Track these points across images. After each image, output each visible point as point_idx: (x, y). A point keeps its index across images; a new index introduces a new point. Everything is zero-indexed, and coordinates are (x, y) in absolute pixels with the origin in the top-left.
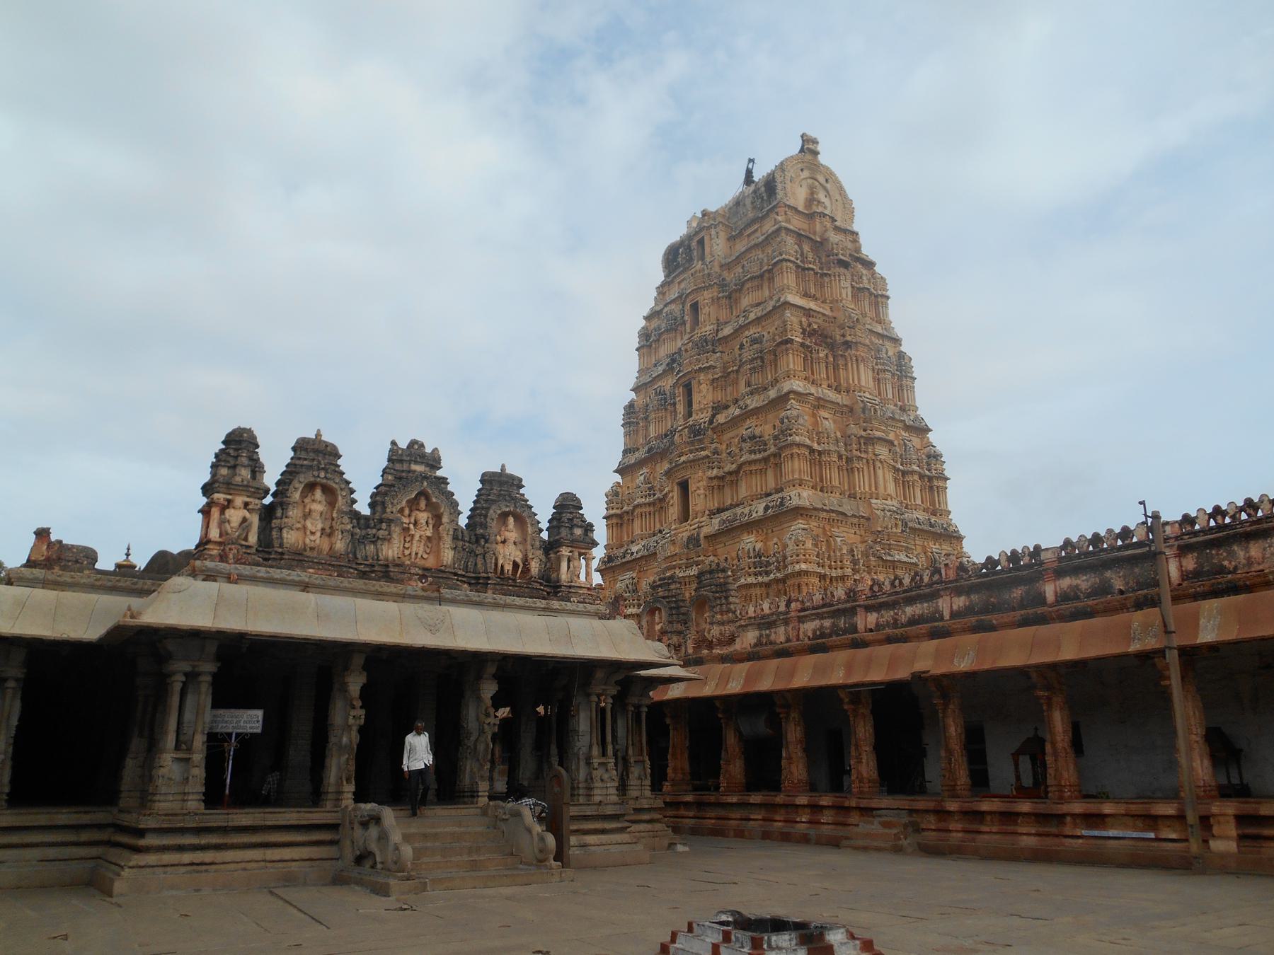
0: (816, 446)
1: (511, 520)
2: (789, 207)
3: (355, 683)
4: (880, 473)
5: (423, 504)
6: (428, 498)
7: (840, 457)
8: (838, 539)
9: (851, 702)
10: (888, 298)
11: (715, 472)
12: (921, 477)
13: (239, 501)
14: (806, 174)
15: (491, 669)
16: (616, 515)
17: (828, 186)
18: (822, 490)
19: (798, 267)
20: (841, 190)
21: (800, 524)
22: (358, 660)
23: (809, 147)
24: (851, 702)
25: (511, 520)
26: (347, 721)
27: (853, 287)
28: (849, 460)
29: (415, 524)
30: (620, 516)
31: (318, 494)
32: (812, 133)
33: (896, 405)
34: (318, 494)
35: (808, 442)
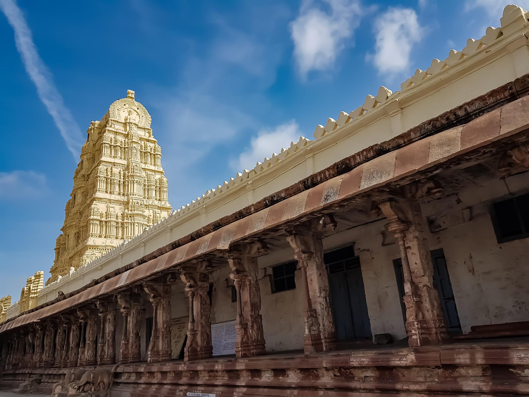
7: (117, 223)
14: (127, 106)
17: (138, 111)
18: (105, 237)
28: (122, 224)
35: (99, 218)
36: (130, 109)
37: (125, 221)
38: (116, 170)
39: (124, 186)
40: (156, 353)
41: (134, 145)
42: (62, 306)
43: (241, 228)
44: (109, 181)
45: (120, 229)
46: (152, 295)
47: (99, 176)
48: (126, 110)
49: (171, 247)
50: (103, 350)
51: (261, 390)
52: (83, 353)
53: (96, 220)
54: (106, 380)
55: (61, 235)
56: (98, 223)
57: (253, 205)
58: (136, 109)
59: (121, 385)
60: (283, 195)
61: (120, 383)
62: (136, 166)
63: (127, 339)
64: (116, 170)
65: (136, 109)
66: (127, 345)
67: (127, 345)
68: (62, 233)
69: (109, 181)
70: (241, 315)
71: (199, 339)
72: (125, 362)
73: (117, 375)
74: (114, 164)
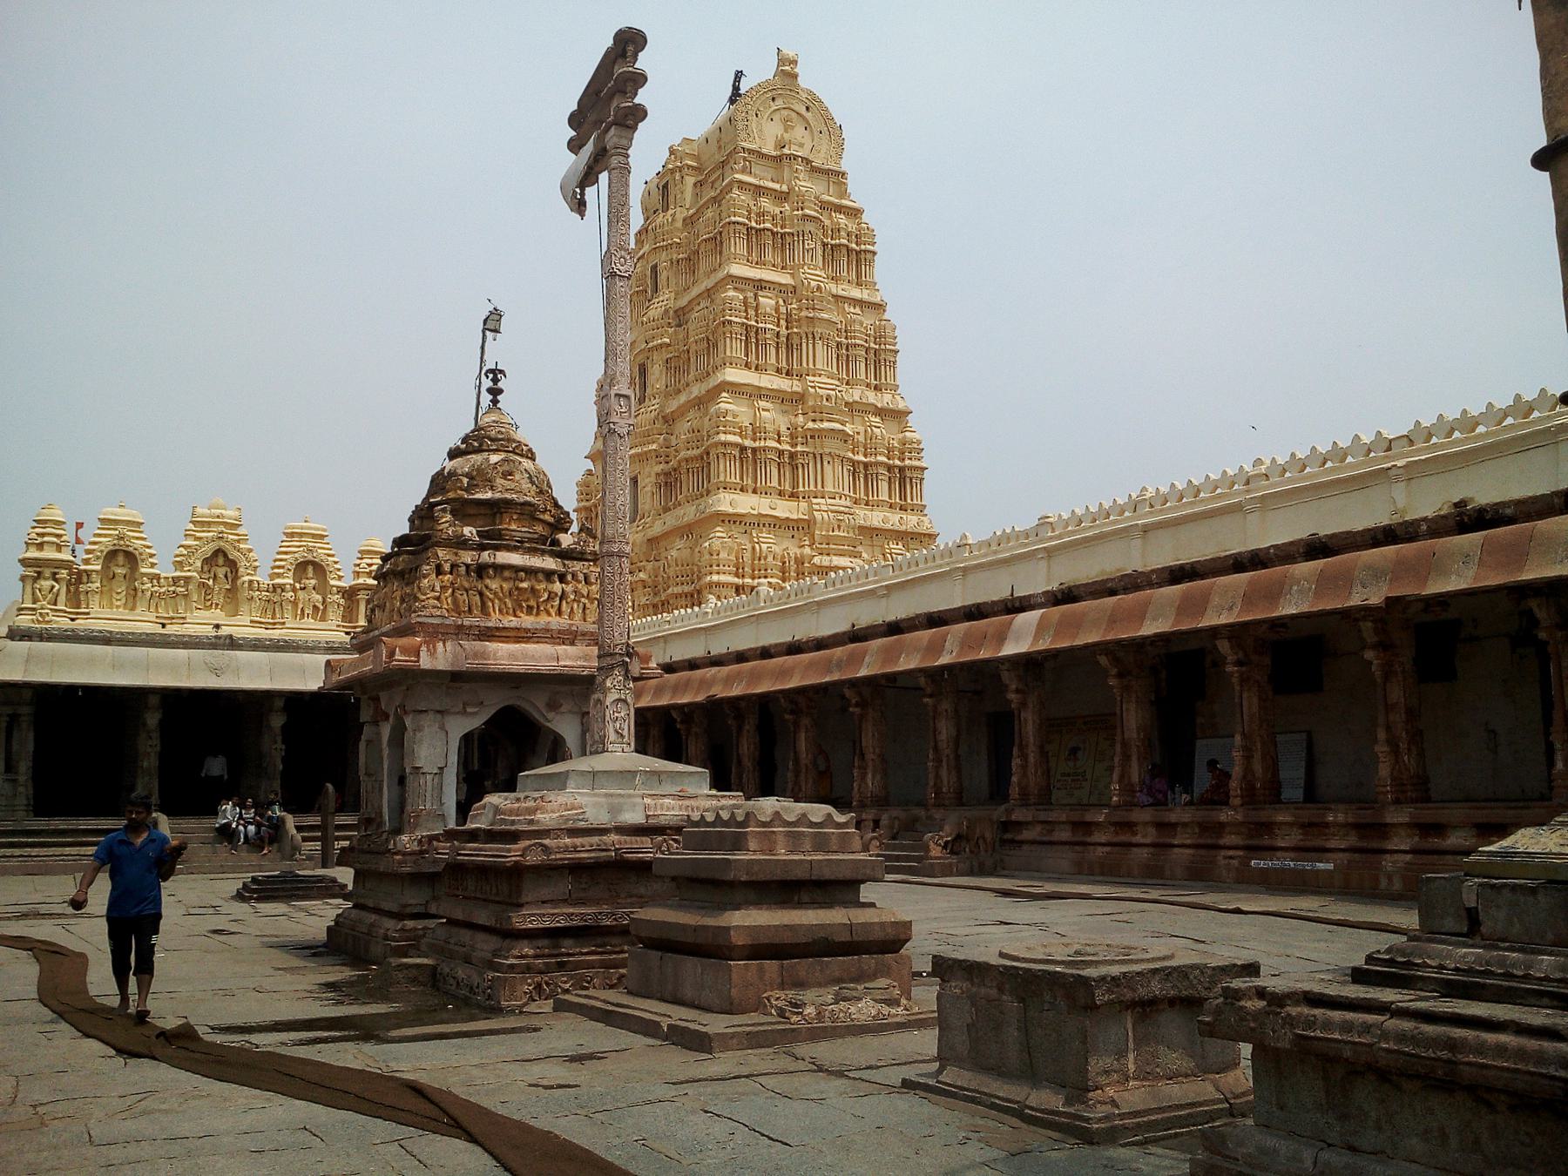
0: (748, 443)
1: (310, 569)
2: (750, 151)
3: (152, 719)
4: (828, 468)
5: (221, 561)
6: (225, 555)
8: (764, 546)
9: (682, 722)
10: (874, 253)
11: (658, 468)
12: (890, 468)
13: (47, 572)
14: (779, 103)
15: (279, 703)
16: (586, 508)
17: (808, 115)
18: (754, 491)
19: (749, 229)
20: (827, 119)
21: (720, 531)
22: (154, 700)
23: (787, 71)
24: (682, 722)
25: (310, 569)
26: (149, 751)
27: (824, 245)
29: (215, 577)
30: (588, 509)
31: (121, 559)
32: (789, 52)
33: (868, 385)
34: (121, 559)
35: (737, 439)
36: (785, 113)
37: (799, 448)
38: (767, 302)
39: (789, 347)
40: (1128, 789)
41: (810, 227)
42: (525, 656)
43: (1400, 569)
44: (752, 336)
45: (788, 469)
46: (1114, 671)
47: (730, 322)
48: (776, 117)
49: (1166, 575)
50: (937, 776)
51: (1449, 857)
52: (863, 777)
53: (731, 444)
54: (988, 835)
55: (589, 473)
56: (736, 452)
57: (1425, 519)
58: (803, 110)
59: (1025, 847)
60: (1508, 511)
61: (1022, 842)
62: (819, 288)
63: (1024, 757)
64: (767, 302)
65: (803, 110)
66: (1024, 767)
67: (1024, 767)
68: (590, 465)
69: (752, 336)
70: (1388, 728)
71: (1258, 768)
72: (1024, 801)
73: (1006, 826)
74: (760, 285)
